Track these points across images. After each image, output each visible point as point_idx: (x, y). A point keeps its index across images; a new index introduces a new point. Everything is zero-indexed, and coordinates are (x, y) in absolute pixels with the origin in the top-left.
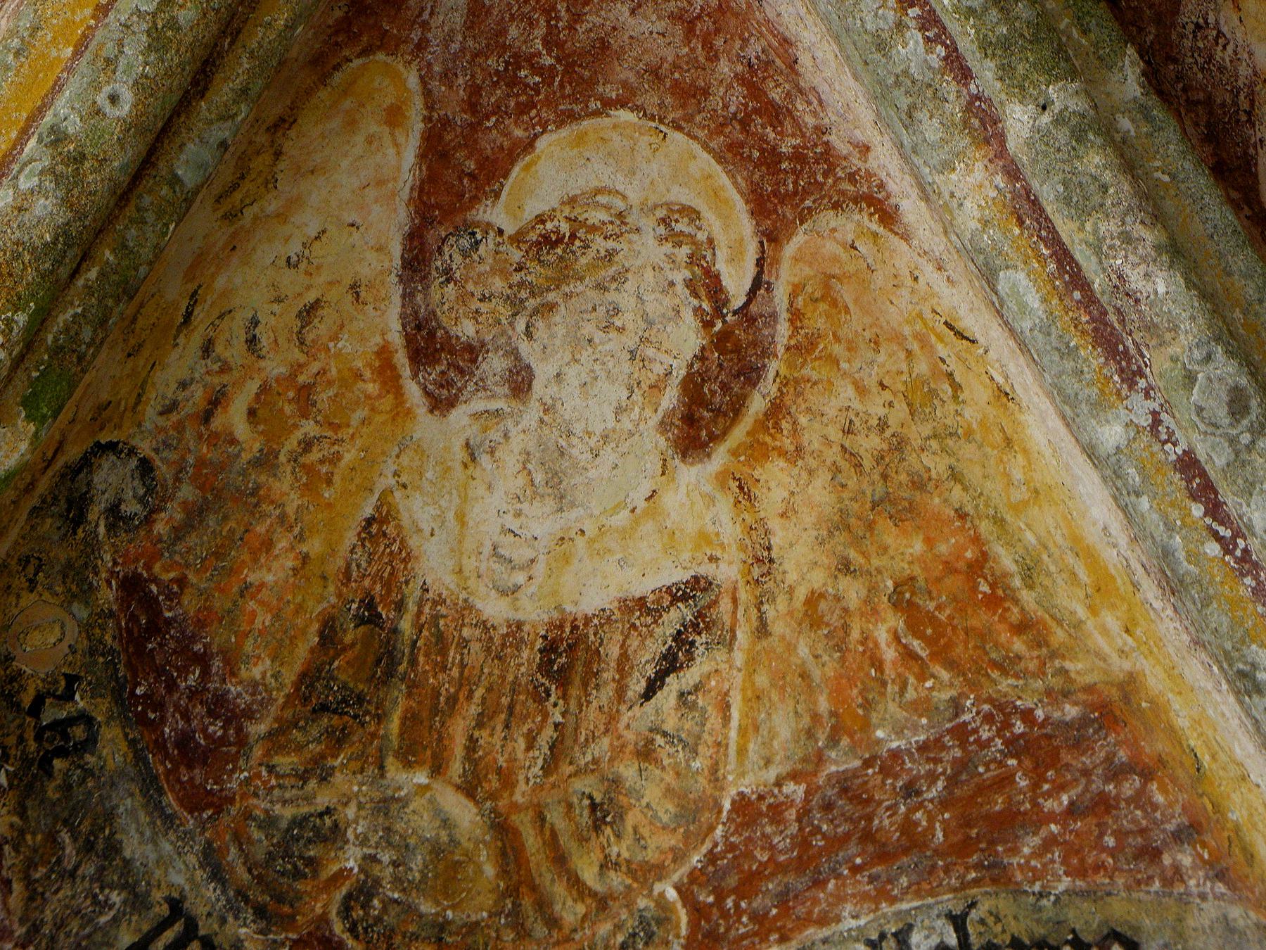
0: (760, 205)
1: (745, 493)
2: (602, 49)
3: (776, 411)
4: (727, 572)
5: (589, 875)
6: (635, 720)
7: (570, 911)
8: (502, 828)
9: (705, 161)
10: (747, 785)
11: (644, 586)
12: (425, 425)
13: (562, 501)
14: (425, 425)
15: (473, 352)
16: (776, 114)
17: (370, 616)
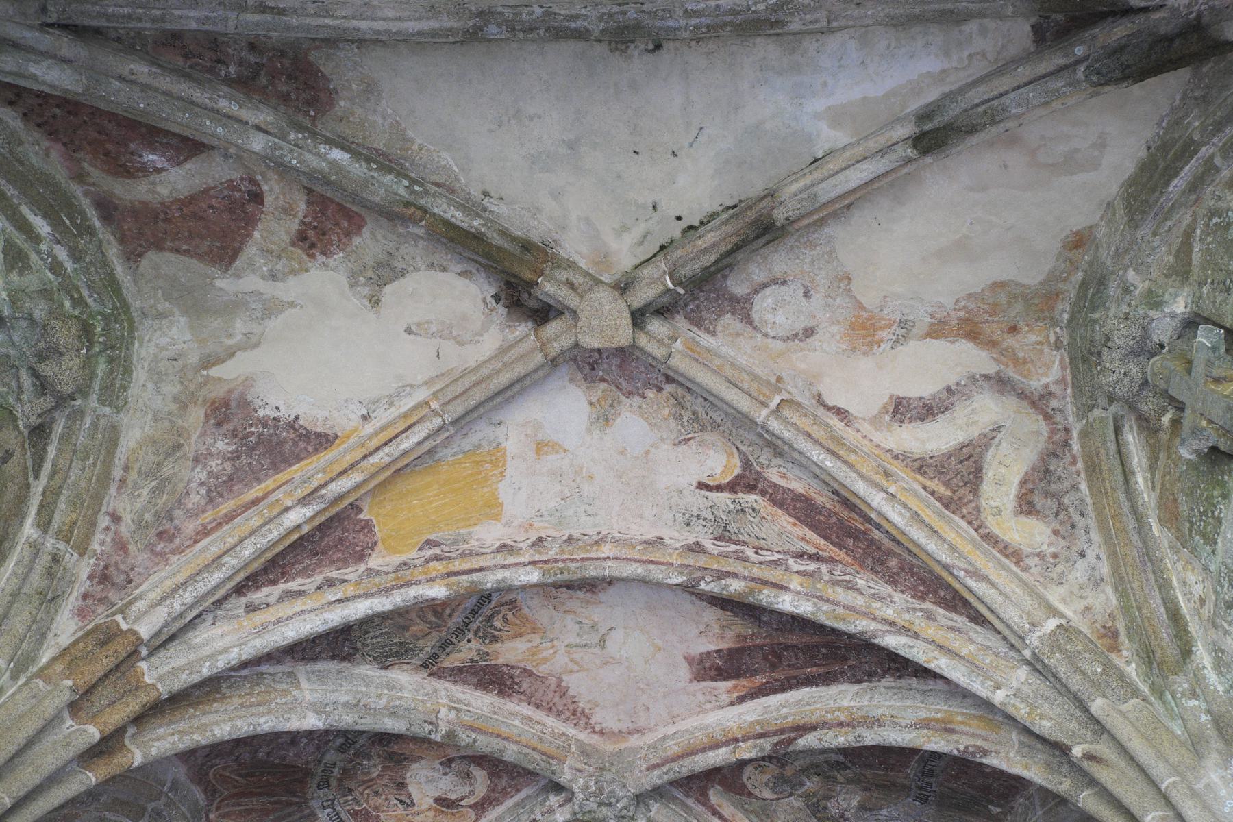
0: (474, 804)
1: (429, 809)
2: (500, 777)
3: (443, 812)
4: (416, 808)
5: (366, 792)
6: (392, 797)
7: (361, 789)
8: (373, 779)
9: (482, 795)
10: (382, 817)
11: (413, 796)
12: (438, 762)
13: (426, 782)
14: (438, 762)
15: (450, 767)
16: (490, 804)
17: (405, 759)
